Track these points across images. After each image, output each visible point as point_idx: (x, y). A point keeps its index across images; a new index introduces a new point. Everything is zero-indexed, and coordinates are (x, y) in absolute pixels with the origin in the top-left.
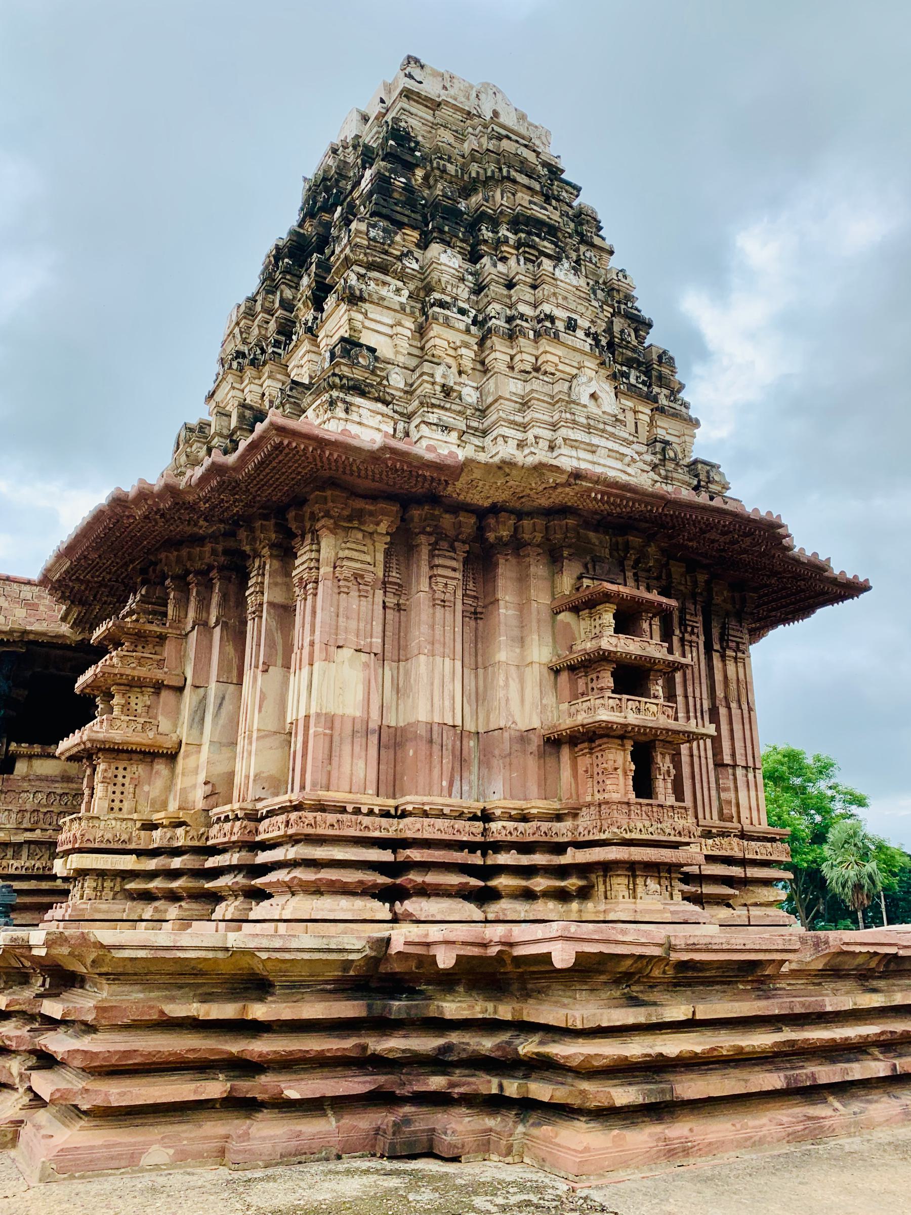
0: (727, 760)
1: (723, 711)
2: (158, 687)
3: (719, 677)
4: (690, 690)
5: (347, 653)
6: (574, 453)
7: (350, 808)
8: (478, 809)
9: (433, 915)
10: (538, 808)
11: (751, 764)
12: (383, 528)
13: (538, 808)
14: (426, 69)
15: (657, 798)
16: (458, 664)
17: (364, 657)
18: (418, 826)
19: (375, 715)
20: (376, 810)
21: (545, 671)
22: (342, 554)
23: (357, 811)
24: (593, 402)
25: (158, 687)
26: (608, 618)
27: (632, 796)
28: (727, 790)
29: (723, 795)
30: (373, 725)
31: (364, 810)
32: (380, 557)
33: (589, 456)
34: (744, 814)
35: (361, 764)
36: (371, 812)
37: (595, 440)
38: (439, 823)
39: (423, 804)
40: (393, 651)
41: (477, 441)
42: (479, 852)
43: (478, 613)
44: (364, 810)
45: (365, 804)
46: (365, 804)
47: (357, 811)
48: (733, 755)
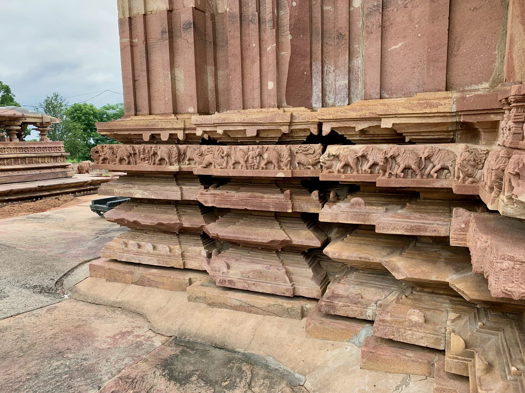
7: (146, 137)
8: (313, 123)
9: (231, 282)
10: (396, 116)
13: (396, 116)
18: (208, 158)
20: (181, 136)
23: (155, 139)
31: (165, 137)
36: (173, 140)
38: (238, 152)
39: (216, 125)
42: (315, 194)
44: (165, 137)
45: (164, 129)
46: (164, 129)
47: (155, 139)
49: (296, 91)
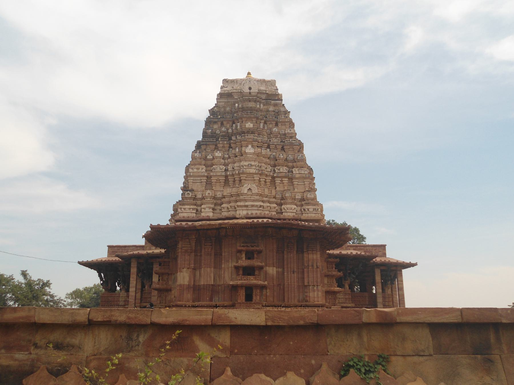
0: (306, 284)
1: (305, 270)
2: (169, 274)
3: (305, 259)
4: (289, 266)
5: (185, 269)
6: (241, 209)
11: (315, 283)
12: (194, 237)
14: (229, 82)
15: (252, 301)
16: (213, 269)
17: (190, 270)
19: (192, 283)
21: (233, 269)
22: (183, 246)
24: (250, 191)
25: (169, 274)
26: (244, 255)
27: (244, 301)
28: (307, 292)
29: (306, 294)
30: (192, 286)
32: (194, 244)
33: (245, 208)
34: (311, 300)
35: (189, 295)
37: (247, 204)
40: (195, 269)
41: (219, 207)
43: (218, 255)
48: (309, 282)
49: (211, 300)
